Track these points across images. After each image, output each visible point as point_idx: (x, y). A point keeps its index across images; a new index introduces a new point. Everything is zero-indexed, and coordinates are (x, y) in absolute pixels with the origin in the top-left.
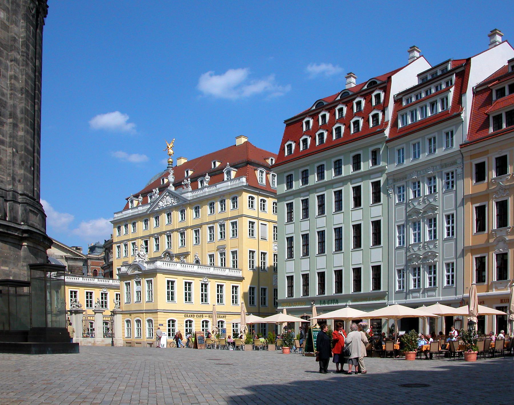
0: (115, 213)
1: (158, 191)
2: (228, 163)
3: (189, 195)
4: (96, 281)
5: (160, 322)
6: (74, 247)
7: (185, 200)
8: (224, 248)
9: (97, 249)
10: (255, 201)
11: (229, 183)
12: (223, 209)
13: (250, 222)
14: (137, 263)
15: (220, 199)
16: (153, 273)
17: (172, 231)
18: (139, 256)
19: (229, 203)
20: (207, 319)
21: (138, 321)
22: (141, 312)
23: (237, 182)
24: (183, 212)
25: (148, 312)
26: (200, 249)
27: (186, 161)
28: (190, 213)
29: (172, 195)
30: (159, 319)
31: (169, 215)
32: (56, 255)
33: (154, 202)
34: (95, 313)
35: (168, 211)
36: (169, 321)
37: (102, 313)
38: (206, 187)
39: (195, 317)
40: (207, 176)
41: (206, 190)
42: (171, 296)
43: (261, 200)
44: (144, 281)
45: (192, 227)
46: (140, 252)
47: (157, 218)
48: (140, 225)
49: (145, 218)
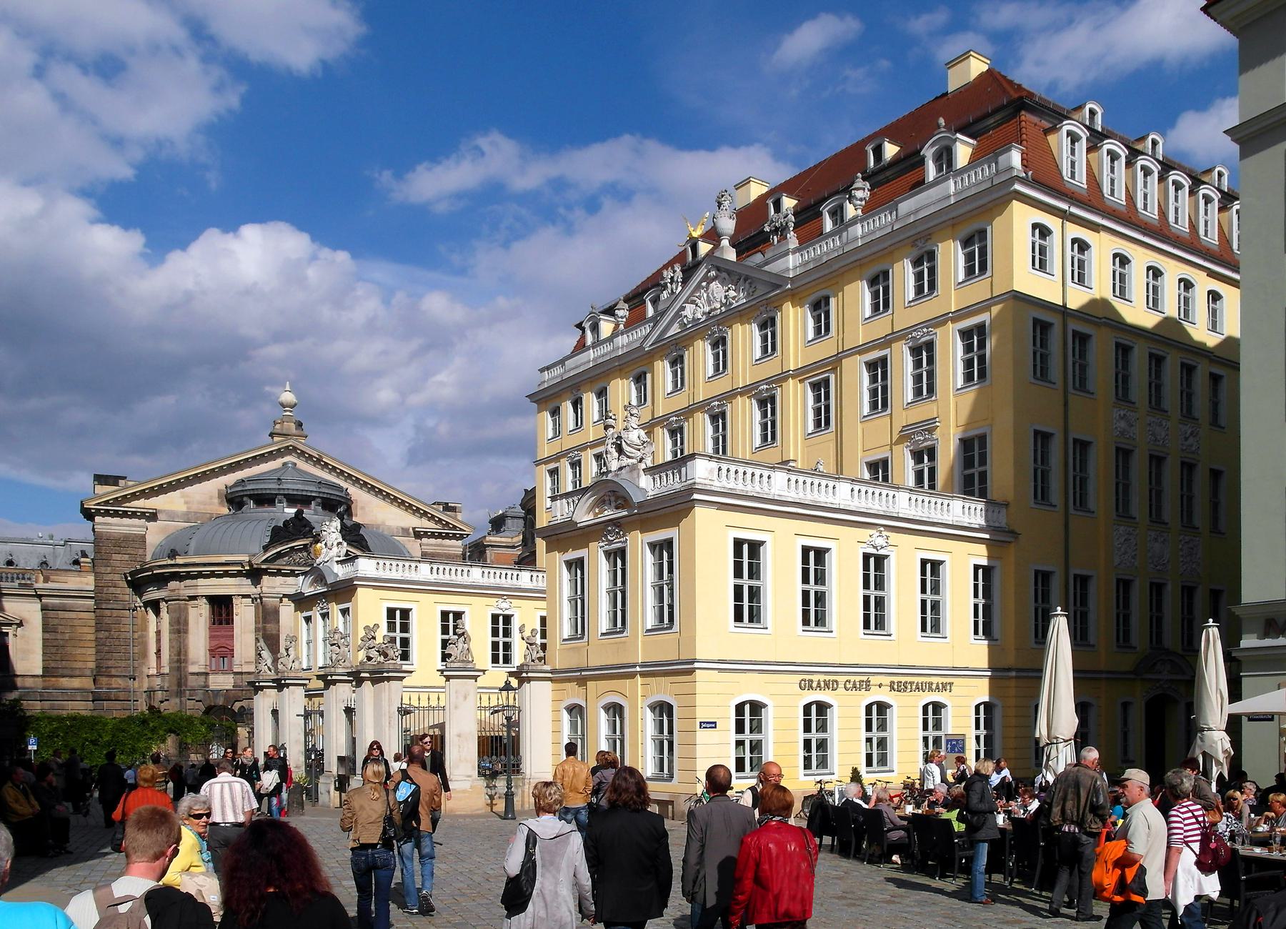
0: (542, 370)
1: (679, 275)
2: (942, 121)
3: (792, 263)
4: (476, 575)
5: (702, 715)
6: (439, 504)
7: (777, 282)
8: (931, 431)
9: (509, 522)
10: (1055, 242)
11: (951, 186)
12: (926, 285)
13: (1036, 322)
14: (610, 477)
15: (916, 253)
16: (677, 506)
17: (730, 395)
18: (620, 450)
19: (951, 256)
20: (884, 696)
21: (615, 710)
22: (622, 672)
23: (986, 171)
24: (768, 324)
25: (654, 670)
26: (832, 445)
27: (765, 190)
28: (795, 321)
29: (725, 272)
30: (699, 700)
31: (719, 342)
32: (389, 527)
33: (663, 314)
34: (448, 678)
35: (715, 331)
36: (740, 709)
37: (475, 678)
38: (854, 221)
39: (841, 690)
40: (859, 183)
41: (858, 230)
42: (748, 607)
43: (1074, 241)
44: (638, 544)
45: (800, 373)
46: (624, 435)
47: (677, 361)
48: (622, 390)
49: (636, 367)
